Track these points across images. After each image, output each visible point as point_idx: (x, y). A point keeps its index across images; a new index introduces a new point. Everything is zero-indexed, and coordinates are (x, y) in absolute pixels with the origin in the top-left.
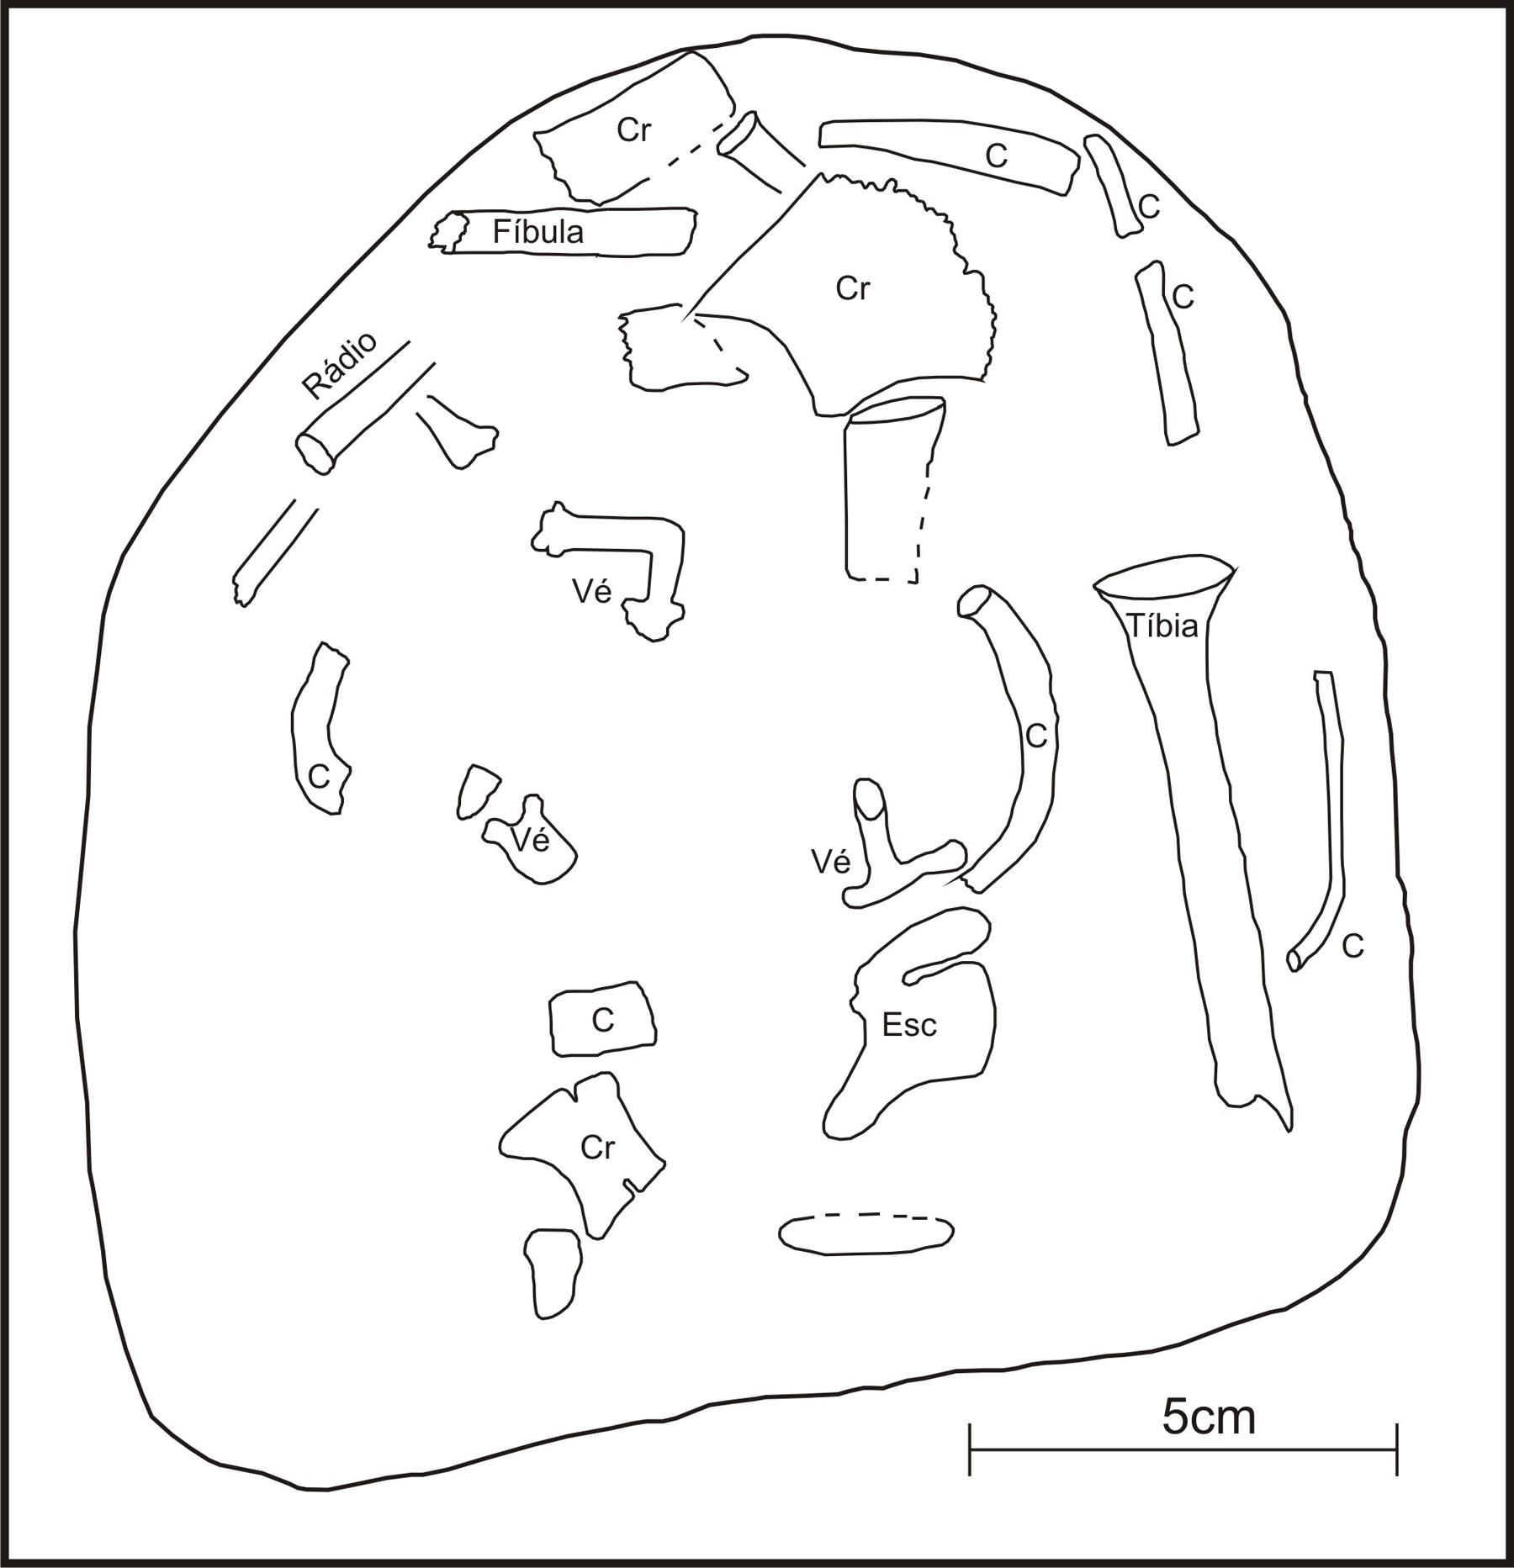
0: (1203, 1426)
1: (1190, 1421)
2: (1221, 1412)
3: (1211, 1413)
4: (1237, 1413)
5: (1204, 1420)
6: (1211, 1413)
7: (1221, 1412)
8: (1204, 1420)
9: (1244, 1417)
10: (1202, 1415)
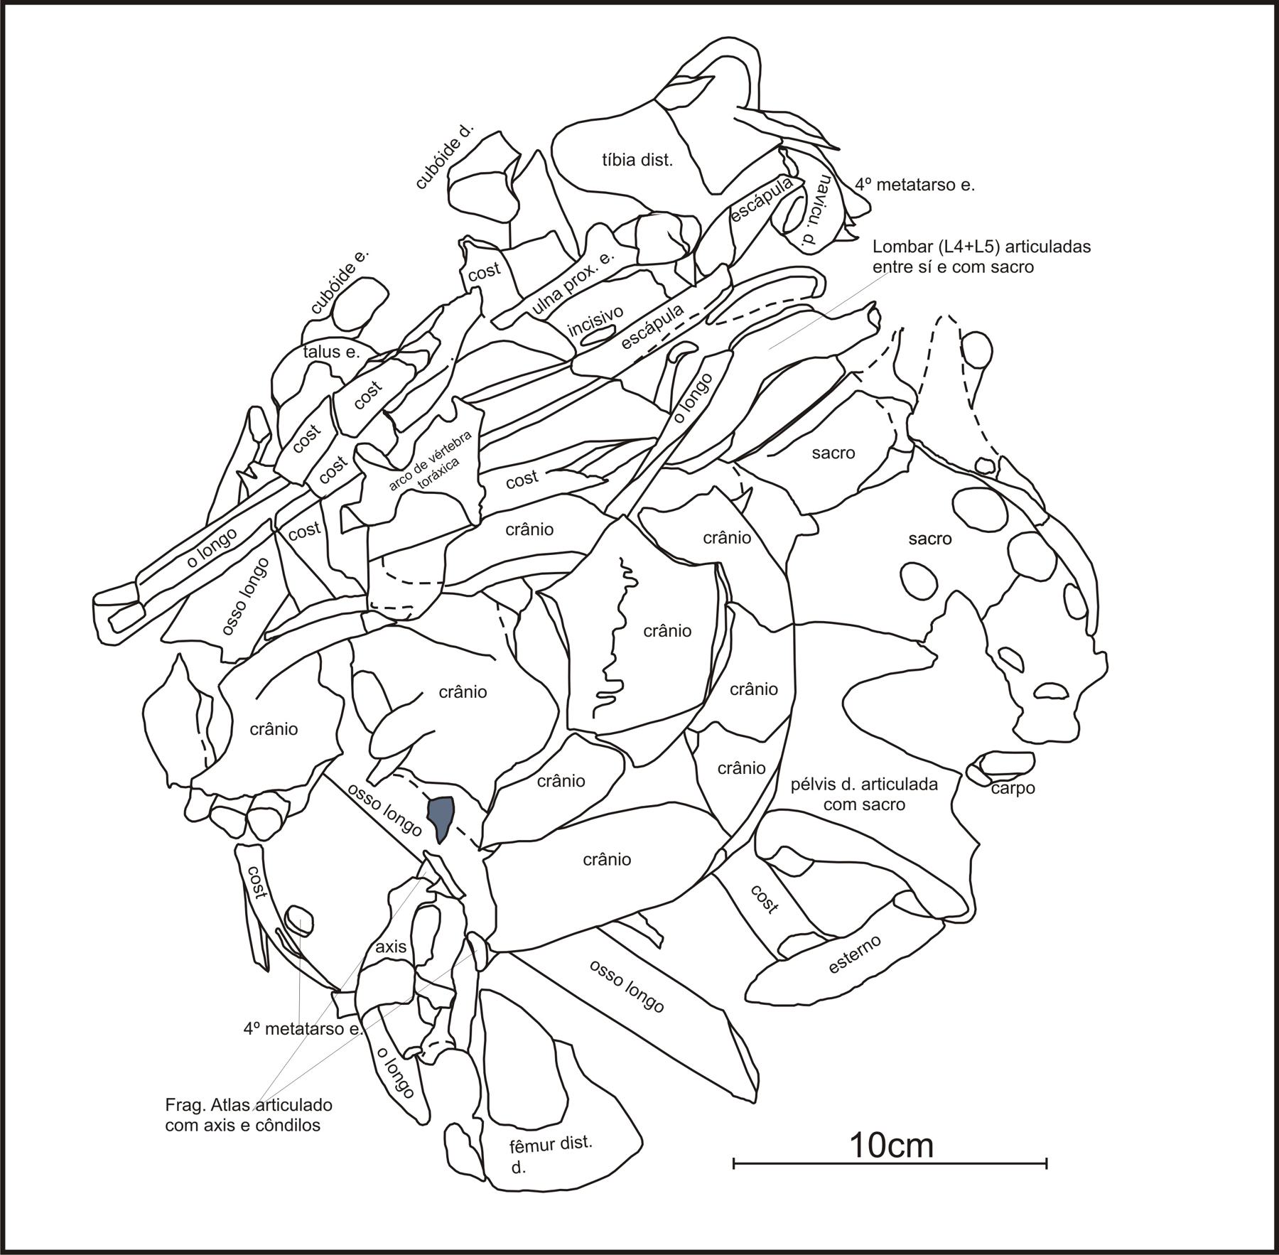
0: (896, 1152)
2: (909, 1142)
3: (902, 1143)
4: (920, 1143)
5: (897, 1148)
6: (902, 1143)
7: (909, 1142)
8: (897, 1148)
9: (925, 1145)
10: (896, 1144)
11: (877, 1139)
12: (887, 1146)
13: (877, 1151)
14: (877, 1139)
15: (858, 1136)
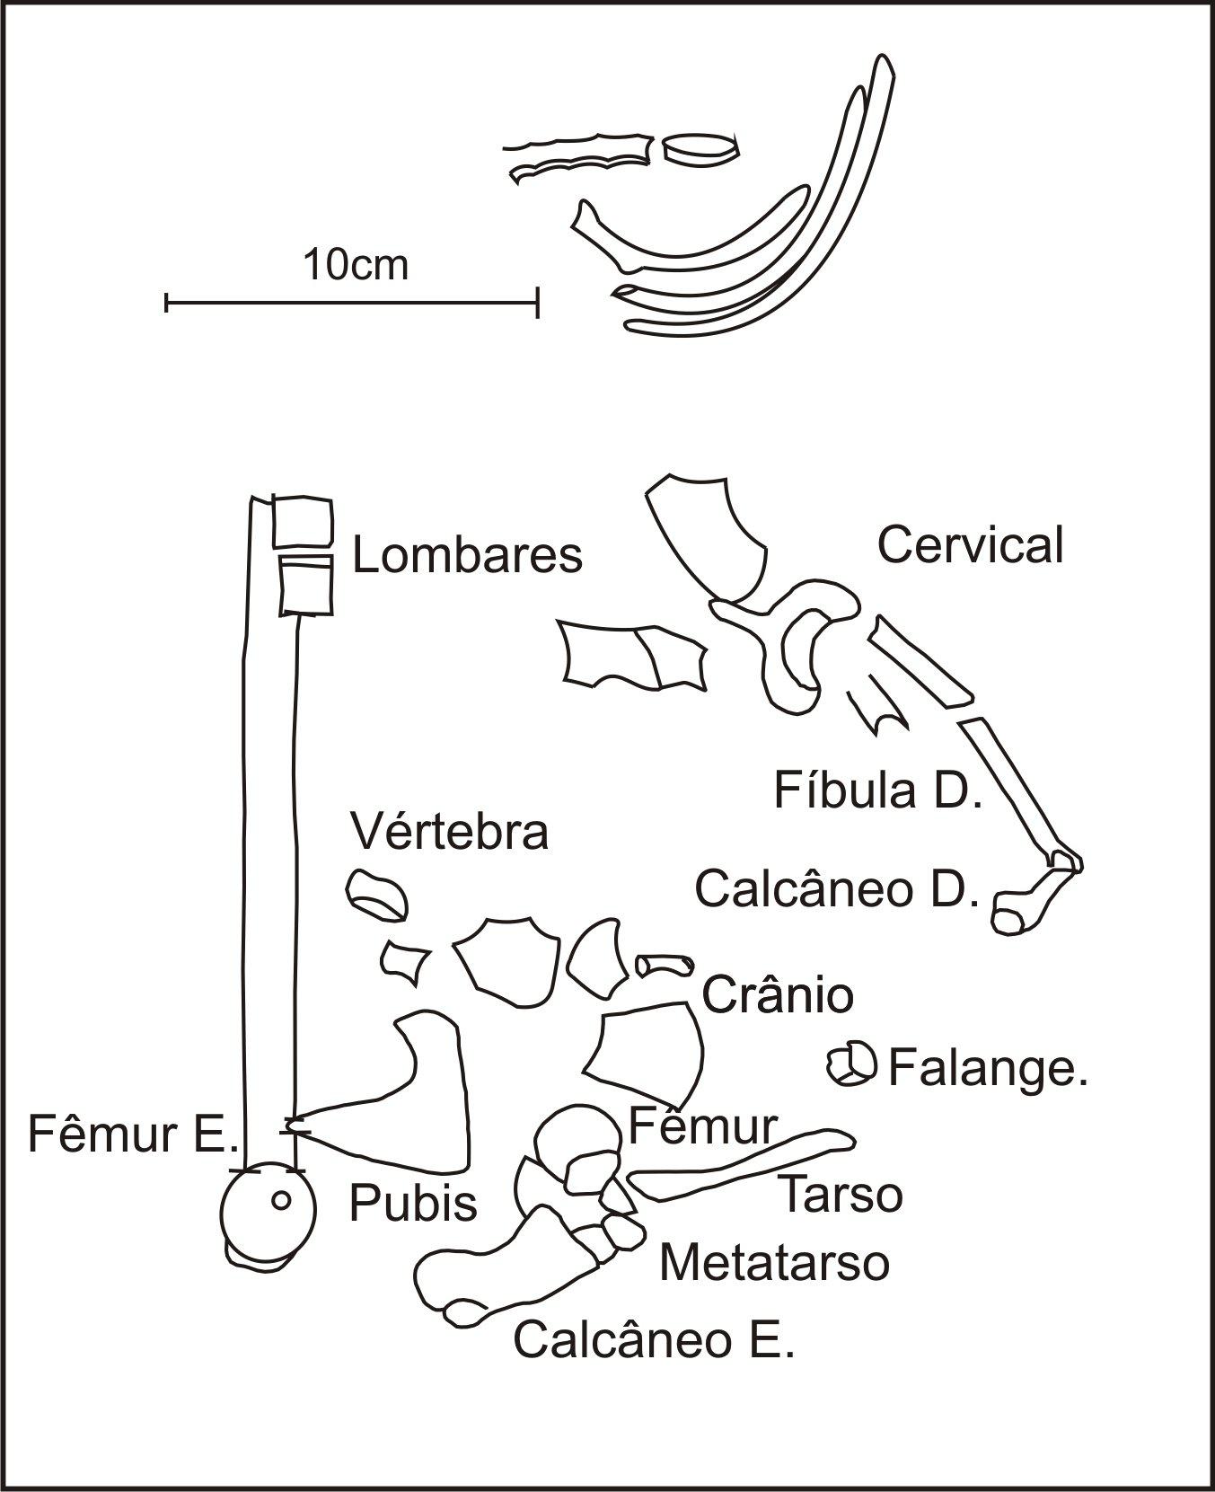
0: (362, 271)
1: (350, 266)
2: (378, 260)
5: (363, 268)
7: (378, 260)
8: (363, 268)
9: (398, 265)
11: (337, 256)
12: (350, 266)
13: (338, 268)
14: (337, 256)
15: (314, 252)
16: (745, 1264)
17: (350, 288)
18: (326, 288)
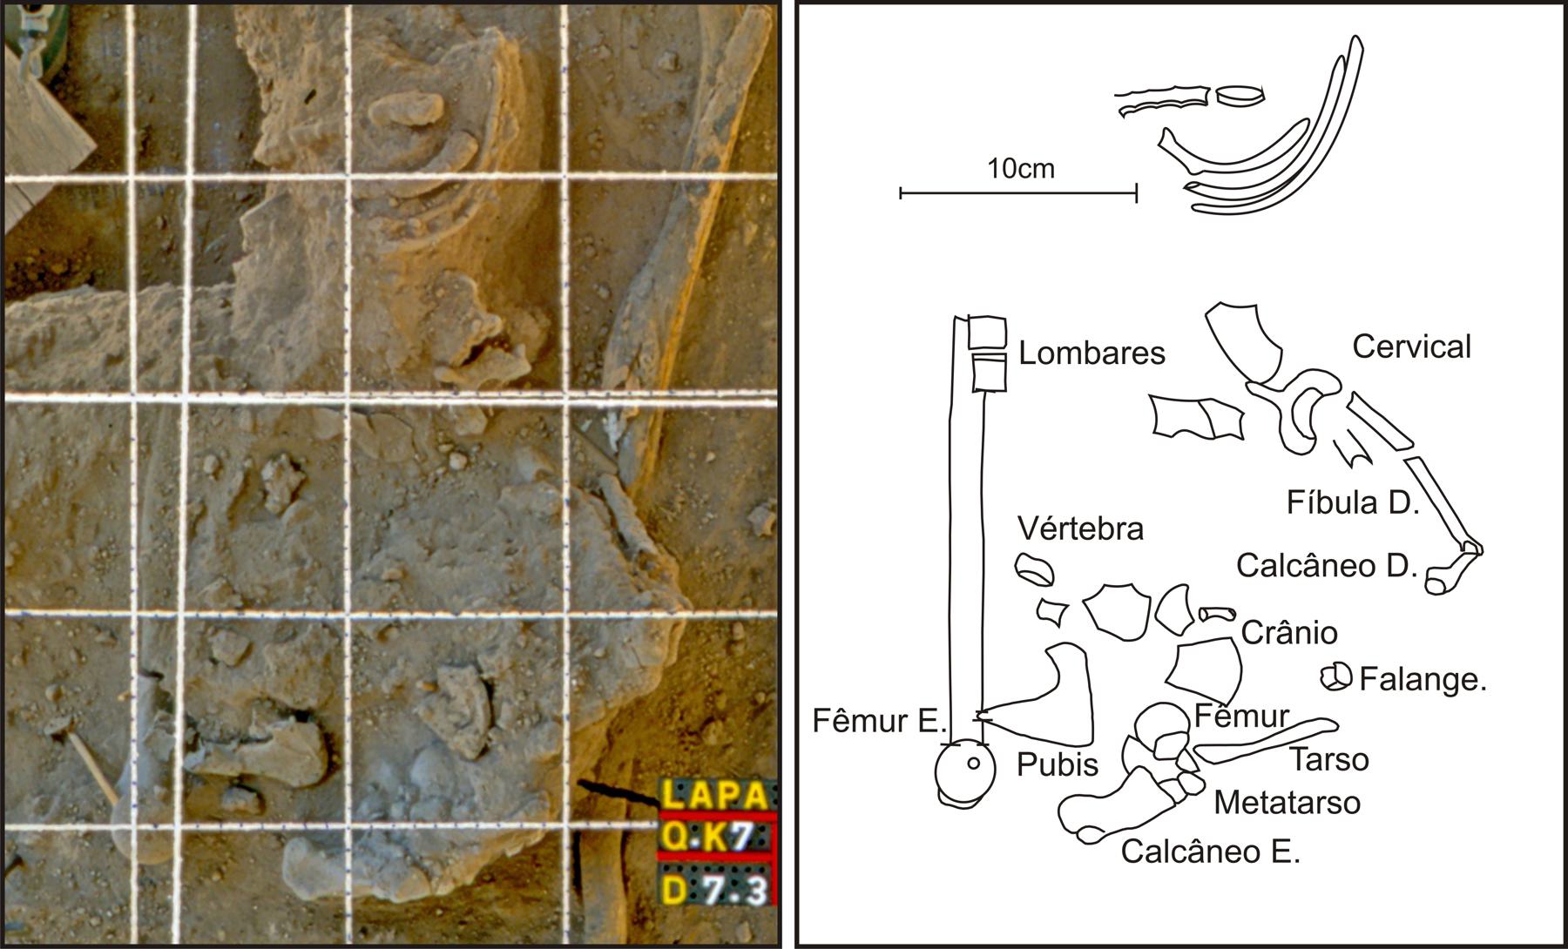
1: (1018, 170)
9: (1048, 169)
11: (1010, 163)
12: (1018, 170)
13: (1010, 172)
14: (1010, 164)
15: (995, 161)
16: (1269, 804)
17: (1017, 184)
18: (1002, 184)
